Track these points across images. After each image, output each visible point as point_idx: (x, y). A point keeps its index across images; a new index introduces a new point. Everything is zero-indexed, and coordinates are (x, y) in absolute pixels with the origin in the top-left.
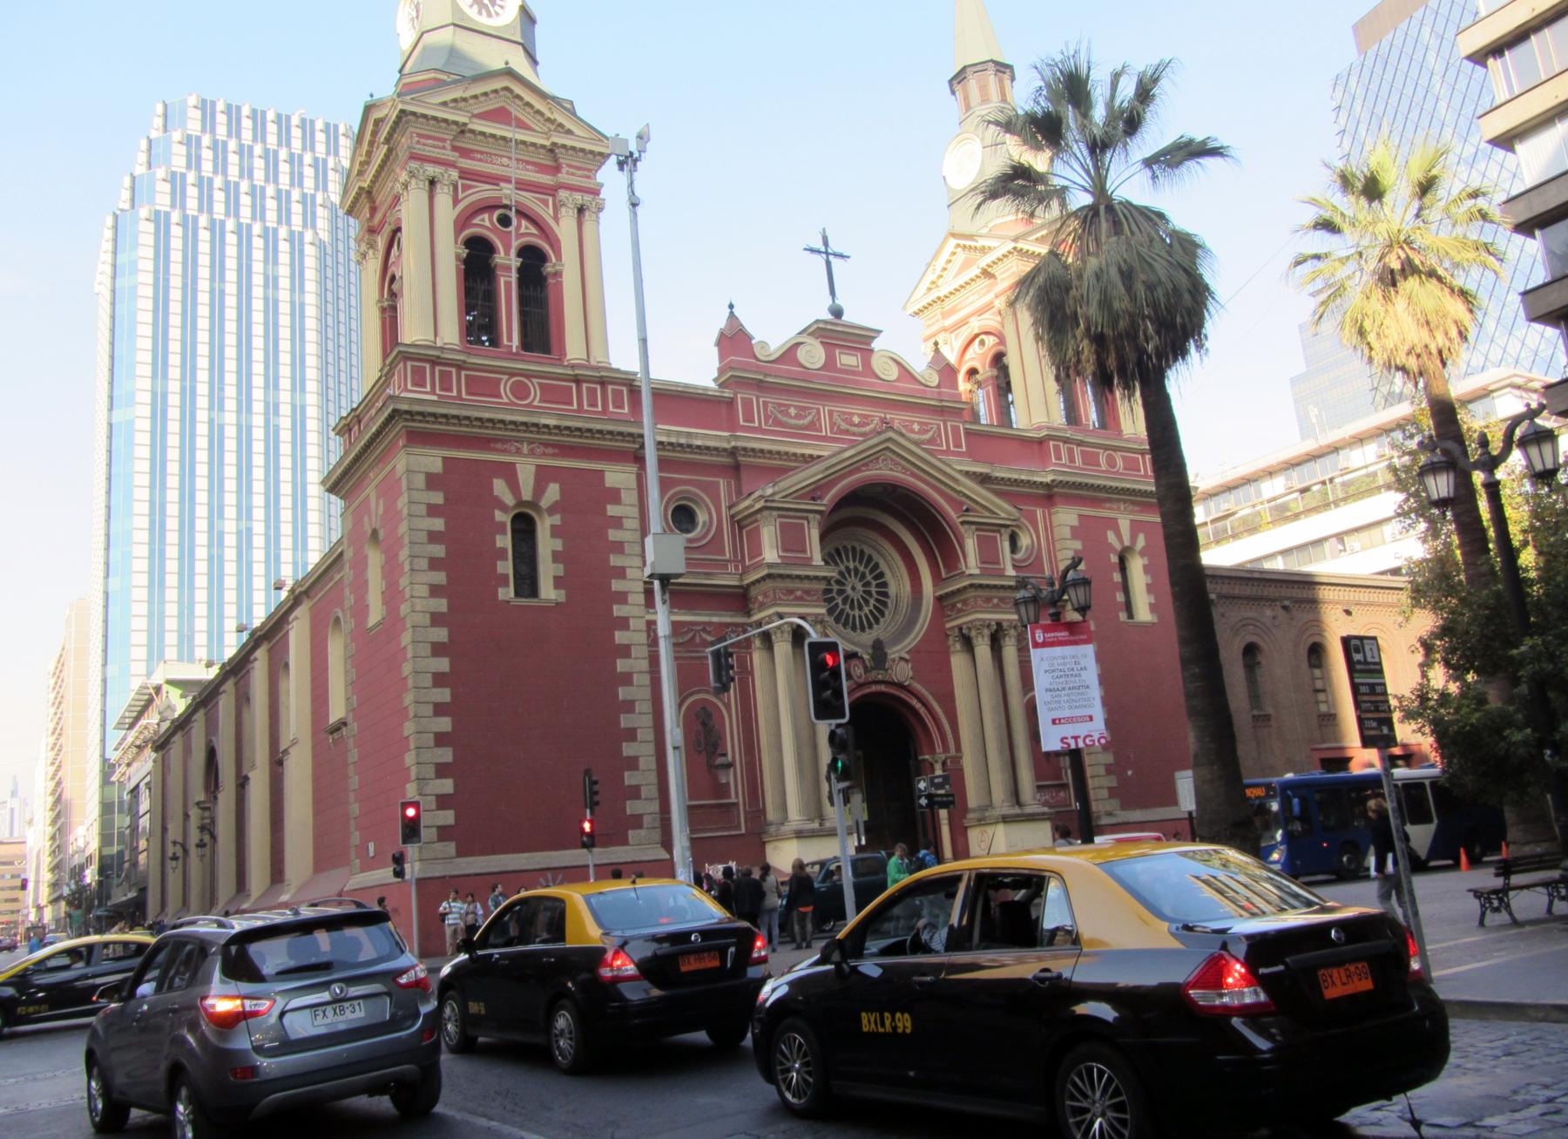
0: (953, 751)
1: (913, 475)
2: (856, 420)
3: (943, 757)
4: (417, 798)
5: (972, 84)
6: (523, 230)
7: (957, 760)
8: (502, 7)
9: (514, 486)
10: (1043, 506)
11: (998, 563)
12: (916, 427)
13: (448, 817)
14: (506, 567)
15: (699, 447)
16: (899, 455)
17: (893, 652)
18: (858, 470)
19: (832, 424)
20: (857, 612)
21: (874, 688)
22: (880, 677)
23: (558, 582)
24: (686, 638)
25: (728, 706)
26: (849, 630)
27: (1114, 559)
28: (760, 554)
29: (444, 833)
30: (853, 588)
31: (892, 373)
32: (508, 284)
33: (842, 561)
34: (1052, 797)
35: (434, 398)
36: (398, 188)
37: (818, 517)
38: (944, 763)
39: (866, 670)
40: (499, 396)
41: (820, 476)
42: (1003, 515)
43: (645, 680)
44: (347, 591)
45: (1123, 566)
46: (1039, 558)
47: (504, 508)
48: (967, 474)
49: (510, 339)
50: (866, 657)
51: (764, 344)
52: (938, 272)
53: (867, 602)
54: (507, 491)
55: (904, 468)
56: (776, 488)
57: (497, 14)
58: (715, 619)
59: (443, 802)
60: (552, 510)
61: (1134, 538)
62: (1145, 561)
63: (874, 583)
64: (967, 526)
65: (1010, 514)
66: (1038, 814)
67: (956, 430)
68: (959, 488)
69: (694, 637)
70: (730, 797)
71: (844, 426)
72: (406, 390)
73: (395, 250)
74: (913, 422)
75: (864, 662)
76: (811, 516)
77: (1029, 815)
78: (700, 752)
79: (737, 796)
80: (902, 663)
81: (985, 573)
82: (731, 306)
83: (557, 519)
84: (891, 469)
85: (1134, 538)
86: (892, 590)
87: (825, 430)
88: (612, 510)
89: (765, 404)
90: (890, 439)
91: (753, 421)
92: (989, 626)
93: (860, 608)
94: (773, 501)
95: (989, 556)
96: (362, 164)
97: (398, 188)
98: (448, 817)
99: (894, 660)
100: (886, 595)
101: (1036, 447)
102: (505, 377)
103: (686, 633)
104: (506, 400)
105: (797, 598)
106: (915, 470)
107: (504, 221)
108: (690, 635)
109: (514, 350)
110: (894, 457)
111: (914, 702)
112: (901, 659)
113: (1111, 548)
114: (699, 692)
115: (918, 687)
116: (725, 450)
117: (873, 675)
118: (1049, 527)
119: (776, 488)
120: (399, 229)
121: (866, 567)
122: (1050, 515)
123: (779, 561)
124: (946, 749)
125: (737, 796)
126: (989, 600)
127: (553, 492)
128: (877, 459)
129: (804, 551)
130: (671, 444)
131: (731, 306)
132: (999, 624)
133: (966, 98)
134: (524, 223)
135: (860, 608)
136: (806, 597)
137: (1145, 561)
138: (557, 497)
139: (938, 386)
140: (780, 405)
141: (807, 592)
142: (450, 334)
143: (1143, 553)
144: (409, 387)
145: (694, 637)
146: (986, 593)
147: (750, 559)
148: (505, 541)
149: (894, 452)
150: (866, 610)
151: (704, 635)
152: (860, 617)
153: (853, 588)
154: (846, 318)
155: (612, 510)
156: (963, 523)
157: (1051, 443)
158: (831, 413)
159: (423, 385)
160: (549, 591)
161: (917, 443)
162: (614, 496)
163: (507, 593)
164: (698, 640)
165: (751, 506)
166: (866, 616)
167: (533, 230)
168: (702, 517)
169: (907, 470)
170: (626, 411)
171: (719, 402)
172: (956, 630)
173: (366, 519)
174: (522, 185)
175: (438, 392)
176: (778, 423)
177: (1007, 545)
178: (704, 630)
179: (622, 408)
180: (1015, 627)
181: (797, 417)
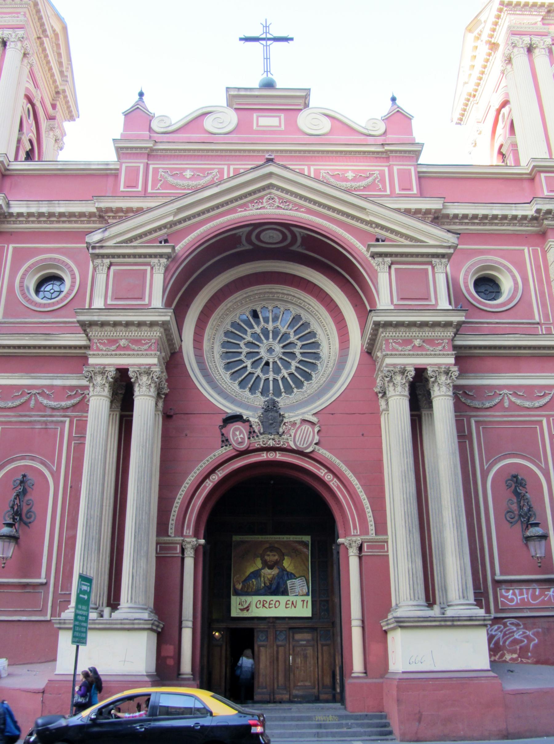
1: (310, 211)
3: (359, 540)
7: (382, 545)
10: (529, 245)
12: (350, 175)
15: (61, 215)
16: (287, 192)
17: (291, 417)
18: (233, 211)
20: (271, 376)
21: (264, 456)
22: (271, 443)
24: (17, 403)
25: (56, 476)
26: (247, 392)
30: (270, 350)
31: (326, 126)
33: (258, 323)
34: (534, 597)
37: (164, 261)
38: (360, 548)
39: (251, 433)
41: (171, 219)
42: (431, 242)
50: (254, 420)
51: (163, 118)
53: (287, 365)
55: (296, 204)
56: (107, 234)
58: (58, 382)
63: (300, 344)
64: (380, 259)
65: (443, 240)
66: (459, 619)
67: (404, 176)
68: (368, 219)
69: (29, 399)
70: (39, 577)
74: (347, 171)
75: (251, 426)
76: (154, 261)
77: (453, 619)
79: (48, 576)
80: (307, 427)
81: (398, 309)
82: (141, 94)
84: (278, 207)
86: (324, 351)
89: (156, 170)
90: (270, 175)
92: (403, 372)
93: (277, 371)
94: (102, 247)
99: (294, 424)
100: (317, 356)
101: (526, 184)
103: (22, 395)
105: (119, 348)
106: (311, 206)
110: (283, 195)
111: (322, 473)
112: (304, 421)
114: (23, 458)
115: (324, 453)
116: (91, 215)
117: (259, 442)
119: (107, 234)
122: (545, 253)
124: (365, 530)
125: (48, 576)
126: (408, 342)
128: (262, 198)
130: (30, 215)
131: (141, 94)
132: (420, 372)
135: (277, 371)
136: (133, 347)
139: (385, 133)
140: (172, 169)
141: (137, 341)
146: (402, 333)
149: (283, 190)
150: (285, 373)
151: (40, 399)
152: (275, 380)
153: (270, 350)
156: (373, 255)
157: (543, 175)
161: (347, 191)
164: (32, 403)
166: (283, 378)
169: (301, 206)
171: (107, 175)
176: (167, 185)
178: (42, 394)
180: (447, 373)
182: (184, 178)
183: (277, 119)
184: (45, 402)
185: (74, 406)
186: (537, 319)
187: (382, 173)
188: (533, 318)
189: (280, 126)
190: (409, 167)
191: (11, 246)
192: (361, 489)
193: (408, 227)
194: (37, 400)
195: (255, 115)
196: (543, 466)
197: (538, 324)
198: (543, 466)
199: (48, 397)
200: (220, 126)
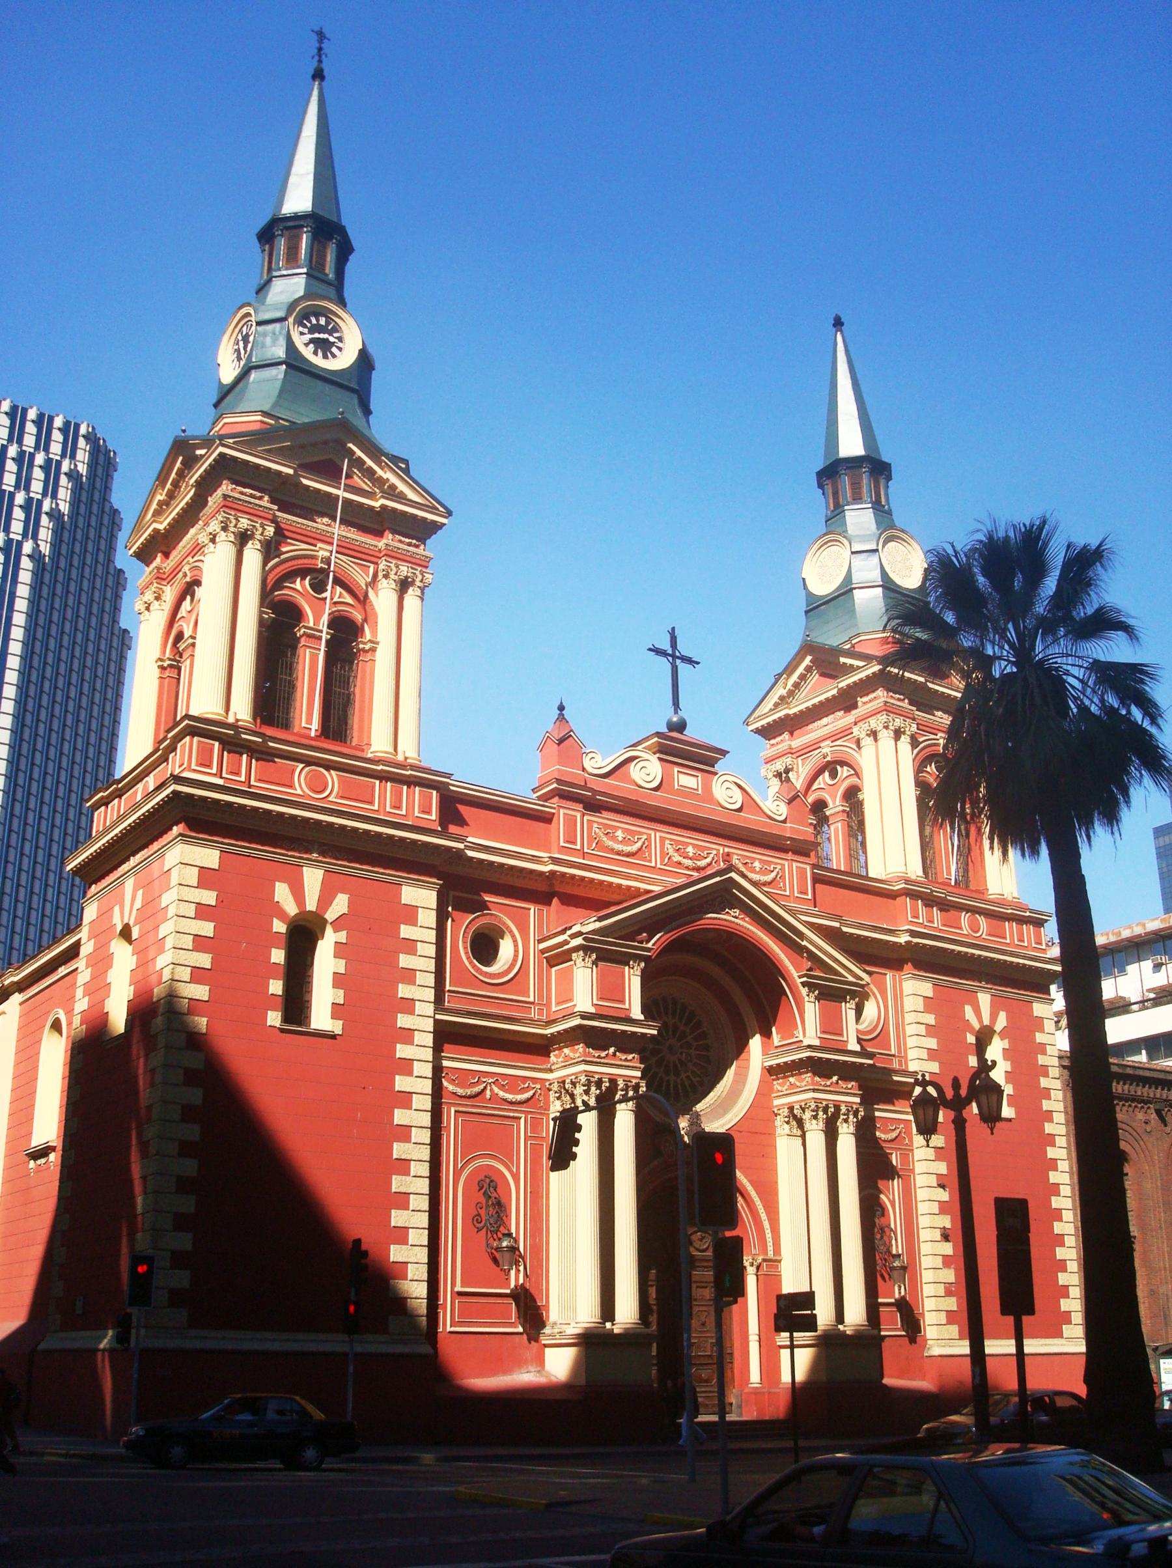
0: (771, 1254)
2: (690, 850)
4: (150, 1252)
5: (846, 481)
6: (336, 599)
8: (340, 349)
9: (298, 893)
11: (841, 1035)
12: (757, 864)
13: (182, 1279)
14: (276, 987)
19: (664, 854)
23: (337, 1011)
27: (971, 1039)
28: (571, 1000)
29: (176, 1298)
32: (314, 659)
35: (221, 782)
36: (203, 538)
40: (291, 786)
42: (851, 979)
43: (425, 1136)
44: (79, 992)
45: (981, 1047)
46: (884, 1031)
47: (281, 914)
48: (812, 926)
49: (309, 721)
52: (789, 686)
54: (291, 898)
57: (334, 356)
59: (179, 1259)
60: (338, 924)
61: (994, 1017)
62: (1005, 1044)
67: (802, 873)
69: (485, 1088)
71: (676, 858)
72: (189, 769)
73: (186, 605)
78: (479, 1230)
82: (561, 708)
83: (342, 936)
85: (994, 1017)
87: (655, 861)
88: (406, 931)
91: (575, 843)
95: (831, 1025)
96: (160, 503)
97: (203, 538)
98: (182, 1279)
102: (301, 766)
104: (299, 792)
107: (319, 587)
108: (482, 1087)
109: (313, 734)
113: (968, 1026)
118: (899, 996)
120: (197, 583)
121: (686, 1025)
123: (593, 1010)
127: (340, 905)
129: (622, 1001)
131: (561, 708)
133: (835, 494)
134: (338, 589)
135: (677, 1074)
137: (1005, 1044)
138: (344, 909)
142: (242, 709)
143: (1003, 1034)
144: (193, 767)
145: (485, 1088)
147: (558, 1004)
148: (278, 956)
151: (496, 1090)
154: (691, 733)
155: (406, 931)
158: (663, 840)
159: (210, 766)
160: (321, 1018)
162: (410, 914)
163: (274, 1018)
164: (488, 1093)
165: (566, 942)
167: (348, 599)
168: (506, 949)
170: (434, 817)
172: (786, 1110)
173: (117, 909)
174: (345, 548)
175: (224, 775)
177: (852, 1014)
179: (429, 813)
181: (624, 841)
182: (614, 838)
183: (694, 780)
184: (501, 1094)
185: (528, 1100)
186: (893, 1052)
187: (783, 869)
188: (890, 1050)
189: (697, 790)
190: (805, 866)
191: (452, 893)
192: (763, 1210)
193: (836, 960)
194: (491, 1090)
195: (676, 769)
196: (891, 1197)
197: (894, 1056)
198: (891, 1197)
199: (502, 1087)
200: (649, 778)
